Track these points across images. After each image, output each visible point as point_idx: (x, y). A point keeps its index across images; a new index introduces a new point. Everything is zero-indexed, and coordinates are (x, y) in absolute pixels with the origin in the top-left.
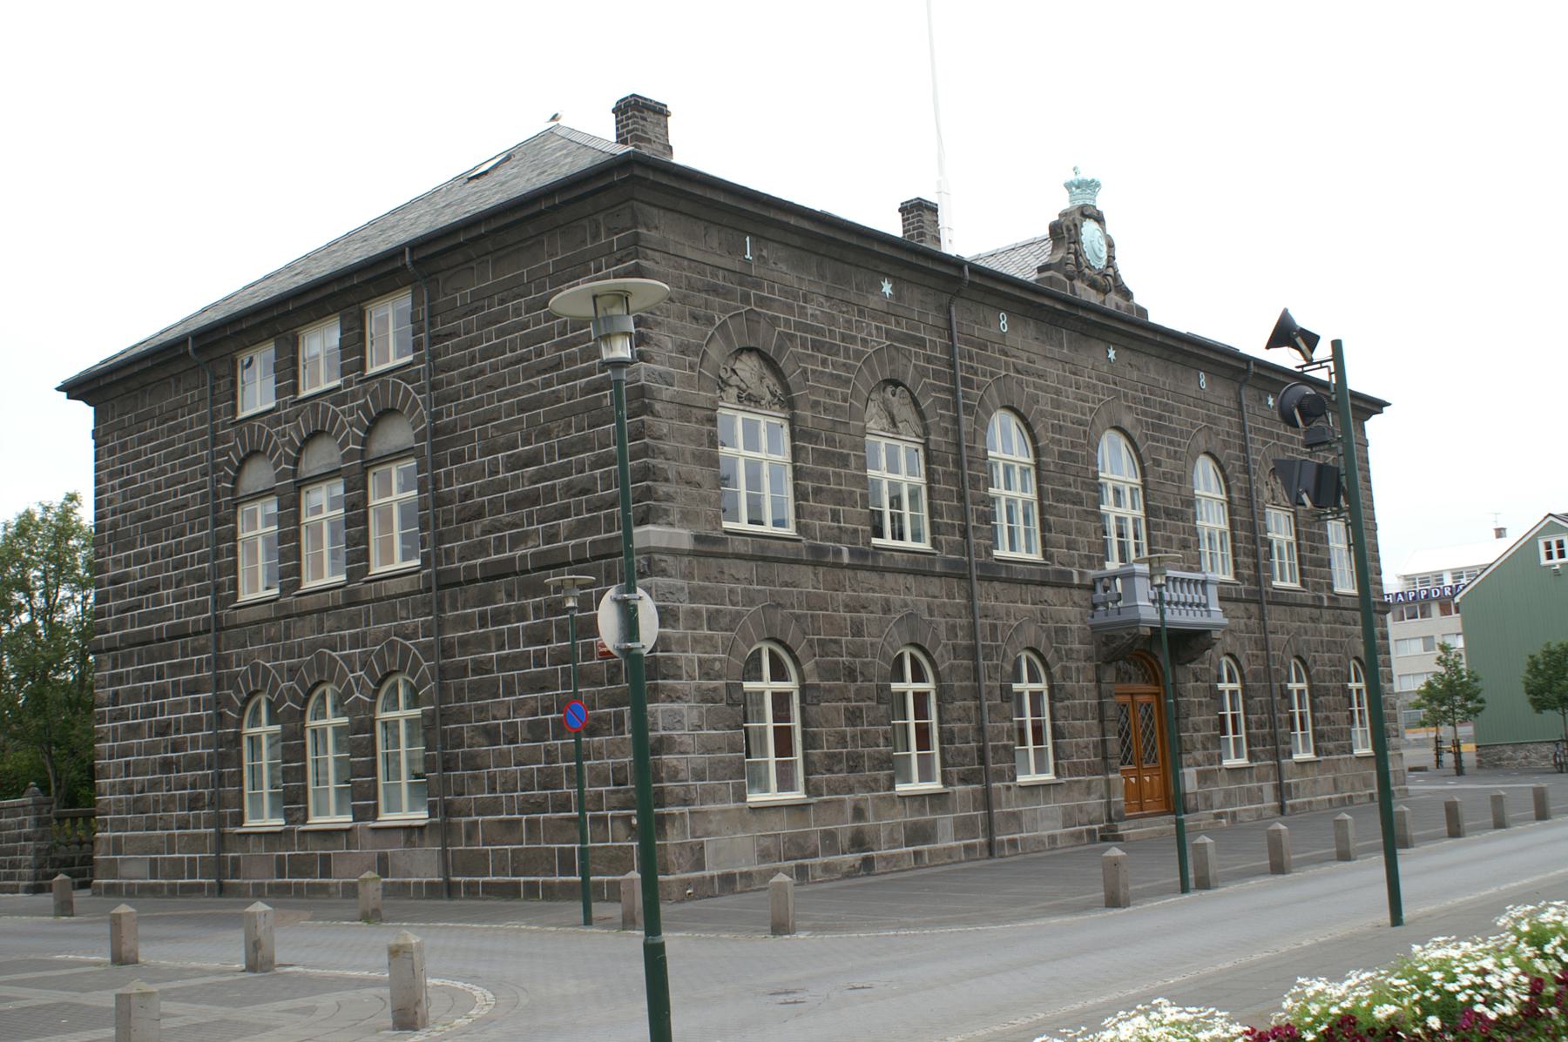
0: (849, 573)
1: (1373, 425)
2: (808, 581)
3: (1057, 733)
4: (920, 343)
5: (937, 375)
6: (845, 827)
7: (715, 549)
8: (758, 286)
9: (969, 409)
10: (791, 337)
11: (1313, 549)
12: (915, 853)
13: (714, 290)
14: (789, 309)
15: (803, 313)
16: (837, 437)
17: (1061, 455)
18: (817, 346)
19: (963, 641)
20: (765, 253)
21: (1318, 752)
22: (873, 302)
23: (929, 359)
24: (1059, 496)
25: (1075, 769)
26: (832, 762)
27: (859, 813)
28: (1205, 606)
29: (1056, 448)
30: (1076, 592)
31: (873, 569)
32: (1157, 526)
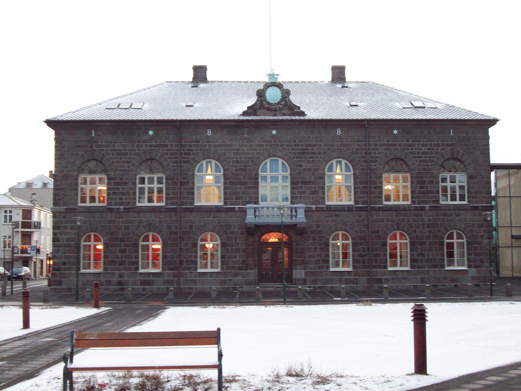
0: (125, 214)
1: (492, 131)
2: (108, 217)
3: (223, 257)
4: (167, 146)
5: (171, 154)
6: (116, 279)
7: (74, 211)
8: (96, 142)
9: (188, 162)
10: (107, 154)
11: (421, 187)
12: (143, 288)
13: (80, 146)
14: (109, 146)
15: (114, 146)
16: (124, 178)
17: (237, 170)
18: (118, 154)
19: (173, 230)
20: (100, 133)
21: (412, 267)
22: (143, 138)
23: (169, 150)
24: (232, 183)
25: (228, 268)
26: (112, 262)
27: (121, 276)
28: (296, 216)
29: (234, 168)
30: (238, 214)
31: (134, 212)
32: (295, 188)
